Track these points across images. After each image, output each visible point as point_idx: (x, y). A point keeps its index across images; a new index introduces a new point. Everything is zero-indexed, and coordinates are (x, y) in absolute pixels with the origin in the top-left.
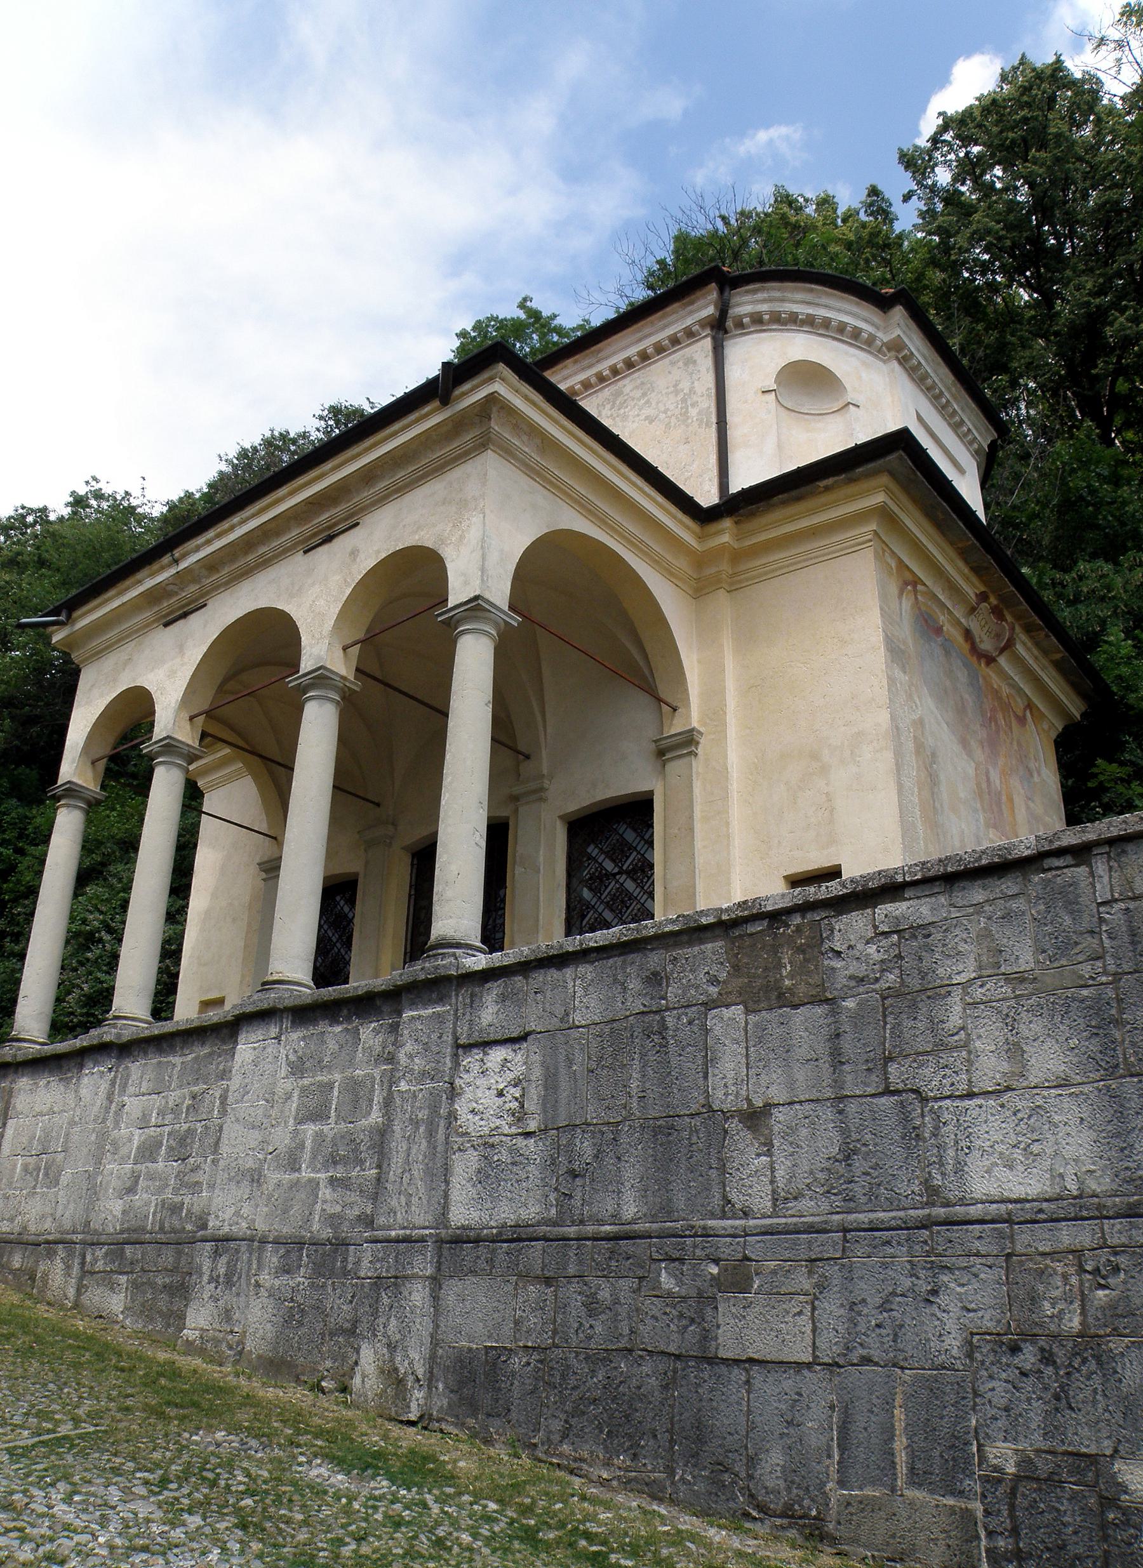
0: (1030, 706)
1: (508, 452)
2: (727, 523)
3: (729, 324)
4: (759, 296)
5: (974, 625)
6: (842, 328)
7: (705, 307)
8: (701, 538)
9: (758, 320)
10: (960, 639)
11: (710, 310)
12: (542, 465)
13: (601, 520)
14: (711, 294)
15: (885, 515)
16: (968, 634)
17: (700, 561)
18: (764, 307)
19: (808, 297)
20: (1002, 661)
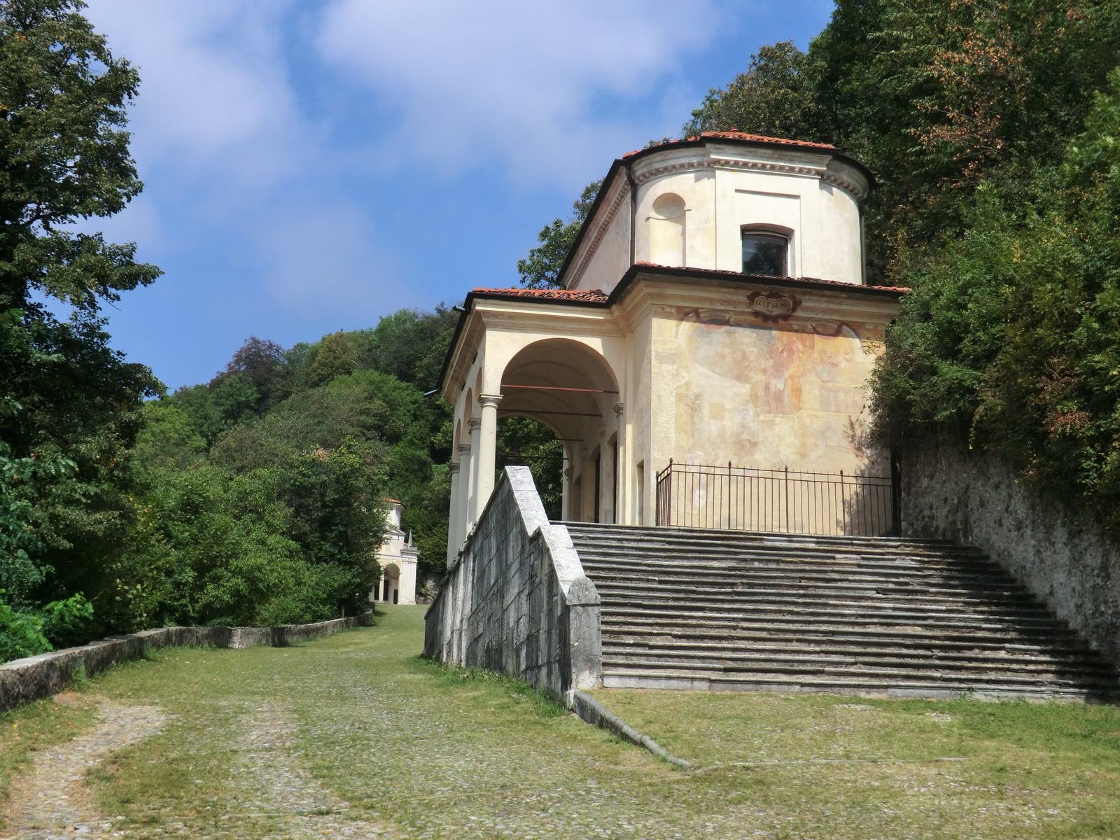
0: (843, 323)
1: (496, 327)
2: (614, 307)
3: (637, 181)
4: (642, 164)
5: (758, 308)
6: (682, 166)
7: (622, 180)
8: (612, 314)
9: (644, 175)
10: (752, 318)
11: (625, 179)
12: (511, 324)
13: (554, 330)
14: (623, 170)
15: (651, 295)
16: (756, 314)
17: (615, 322)
18: (645, 170)
19: (662, 157)
20: (799, 313)
